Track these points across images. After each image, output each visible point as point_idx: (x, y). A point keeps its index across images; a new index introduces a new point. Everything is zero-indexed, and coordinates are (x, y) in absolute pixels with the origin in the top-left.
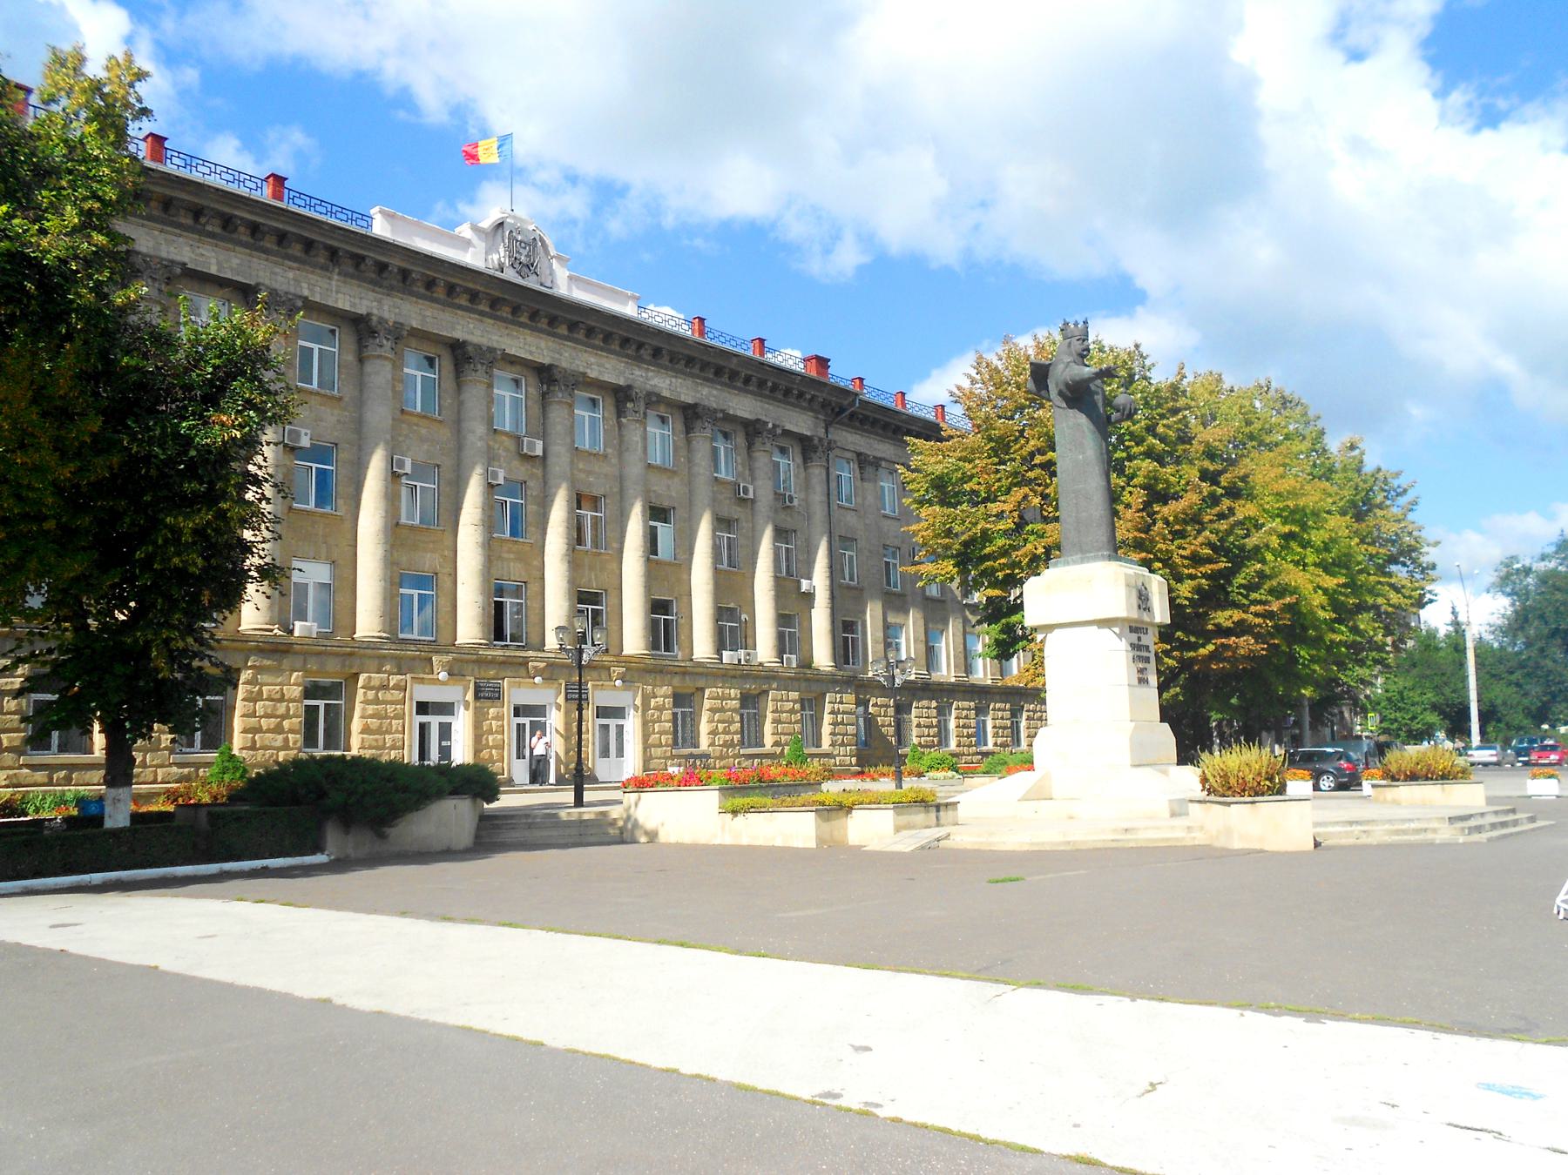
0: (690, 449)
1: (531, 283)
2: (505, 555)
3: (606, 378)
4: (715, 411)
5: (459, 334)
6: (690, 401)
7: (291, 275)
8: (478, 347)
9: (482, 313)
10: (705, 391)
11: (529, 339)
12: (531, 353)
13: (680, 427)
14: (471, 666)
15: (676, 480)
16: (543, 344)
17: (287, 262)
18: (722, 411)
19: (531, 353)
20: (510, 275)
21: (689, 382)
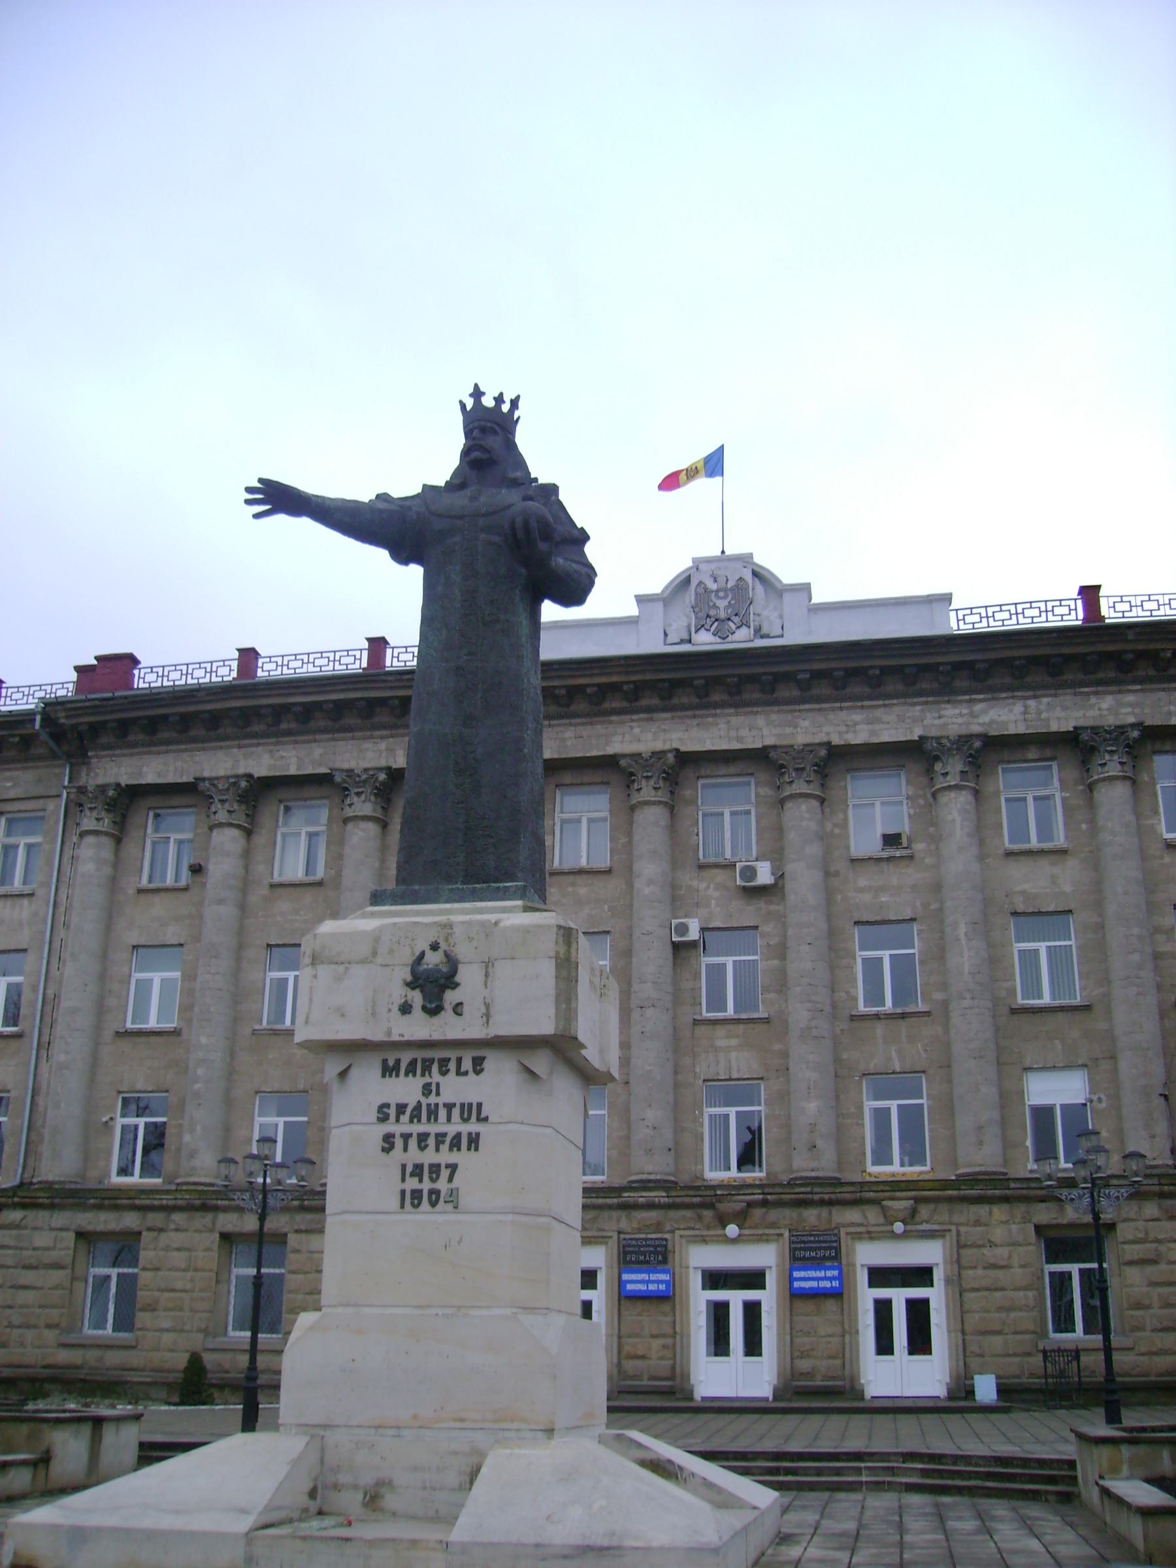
0: (1091, 804)
1: (741, 639)
2: (721, 1043)
3: (886, 737)
4: (1121, 729)
5: (615, 747)
6: (1068, 726)
7: (383, 745)
8: (636, 756)
9: (649, 710)
10: (1107, 702)
11: (735, 720)
12: (739, 739)
13: (1072, 773)
14: (615, 1214)
15: (1072, 863)
16: (760, 721)
17: (377, 733)
18: (1138, 725)
19: (739, 739)
20: (705, 641)
21: (1067, 698)
